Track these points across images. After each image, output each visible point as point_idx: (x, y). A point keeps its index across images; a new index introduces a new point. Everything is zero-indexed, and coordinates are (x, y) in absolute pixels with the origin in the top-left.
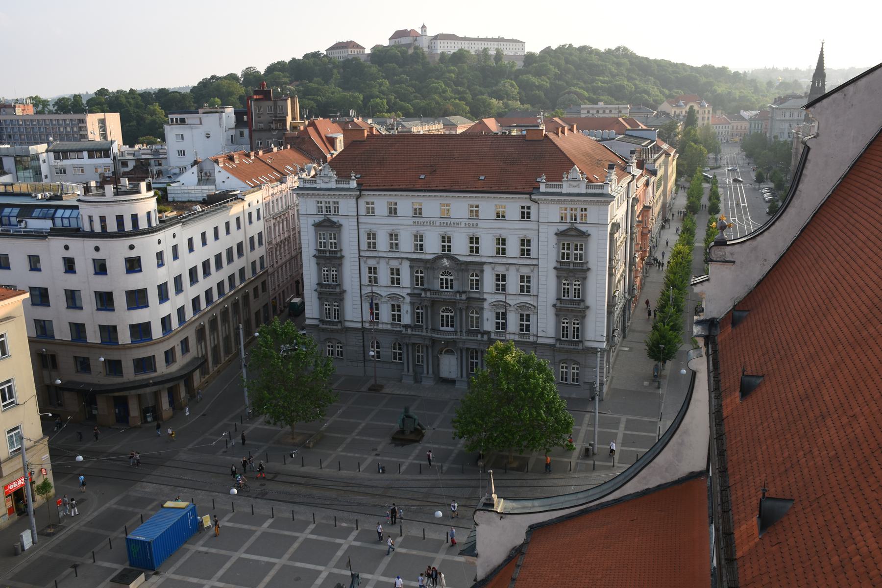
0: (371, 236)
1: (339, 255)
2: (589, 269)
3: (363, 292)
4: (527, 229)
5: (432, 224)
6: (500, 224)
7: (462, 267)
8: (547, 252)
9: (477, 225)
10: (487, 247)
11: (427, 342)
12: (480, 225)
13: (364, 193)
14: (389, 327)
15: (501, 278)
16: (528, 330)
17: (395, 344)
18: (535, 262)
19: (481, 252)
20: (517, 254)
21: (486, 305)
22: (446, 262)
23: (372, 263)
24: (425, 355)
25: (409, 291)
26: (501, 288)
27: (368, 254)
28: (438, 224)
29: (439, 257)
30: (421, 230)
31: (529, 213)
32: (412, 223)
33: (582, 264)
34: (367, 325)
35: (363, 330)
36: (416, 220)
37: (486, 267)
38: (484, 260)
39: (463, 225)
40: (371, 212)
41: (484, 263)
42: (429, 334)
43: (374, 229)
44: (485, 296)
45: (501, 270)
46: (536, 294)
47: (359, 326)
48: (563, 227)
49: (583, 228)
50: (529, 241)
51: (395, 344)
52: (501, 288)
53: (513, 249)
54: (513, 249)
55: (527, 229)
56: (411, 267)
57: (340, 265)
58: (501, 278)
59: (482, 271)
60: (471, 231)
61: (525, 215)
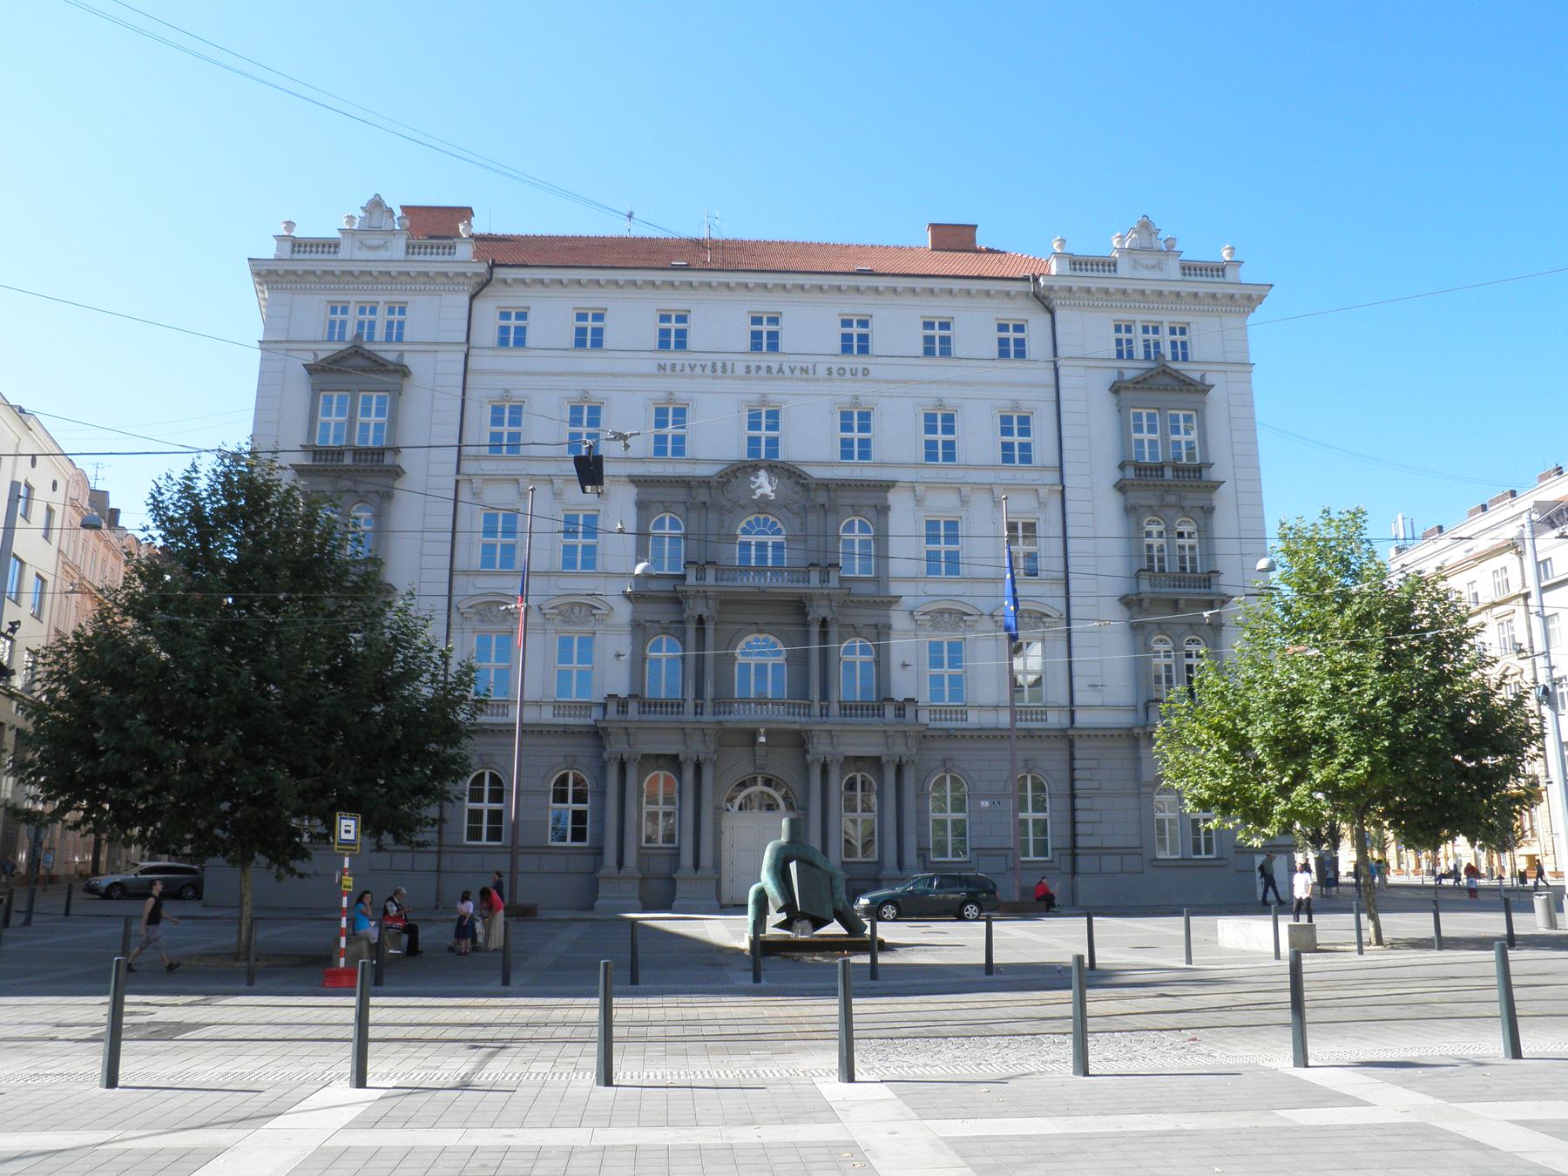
0: (509, 412)
1: (388, 459)
2: (1215, 486)
4: (1023, 384)
5: (721, 370)
6: (937, 368)
7: (814, 498)
8: (1093, 440)
9: (866, 372)
10: (897, 440)
11: (697, 748)
12: (875, 372)
13: (500, 273)
14: (547, 716)
15: (942, 531)
17: (563, 780)
19: (877, 453)
21: (899, 620)
22: (764, 485)
23: (500, 496)
26: (945, 564)
27: (489, 467)
28: (740, 369)
29: (741, 471)
30: (682, 388)
31: (1020, 343)
32: (651, 367)
33: (1199, 469)
36: (668, 357)
37: (893, 497)
38: (886, 475)
39: (822, 371)
40: (513, 337)
41: (888, 485)
44: (895, 589)
45: (942, 505)
48: (1132, 370)
49: (1191, 370)
50: (1024, 421)
52: (945, 564)
53: (978, 439)
54: (978, 439)
55: (1023, 384)
56: (642, 506)
57: (387, 496)
58: (942, 531)
59: (883, 510)
60: (845, 391)
61: (1011, 348)
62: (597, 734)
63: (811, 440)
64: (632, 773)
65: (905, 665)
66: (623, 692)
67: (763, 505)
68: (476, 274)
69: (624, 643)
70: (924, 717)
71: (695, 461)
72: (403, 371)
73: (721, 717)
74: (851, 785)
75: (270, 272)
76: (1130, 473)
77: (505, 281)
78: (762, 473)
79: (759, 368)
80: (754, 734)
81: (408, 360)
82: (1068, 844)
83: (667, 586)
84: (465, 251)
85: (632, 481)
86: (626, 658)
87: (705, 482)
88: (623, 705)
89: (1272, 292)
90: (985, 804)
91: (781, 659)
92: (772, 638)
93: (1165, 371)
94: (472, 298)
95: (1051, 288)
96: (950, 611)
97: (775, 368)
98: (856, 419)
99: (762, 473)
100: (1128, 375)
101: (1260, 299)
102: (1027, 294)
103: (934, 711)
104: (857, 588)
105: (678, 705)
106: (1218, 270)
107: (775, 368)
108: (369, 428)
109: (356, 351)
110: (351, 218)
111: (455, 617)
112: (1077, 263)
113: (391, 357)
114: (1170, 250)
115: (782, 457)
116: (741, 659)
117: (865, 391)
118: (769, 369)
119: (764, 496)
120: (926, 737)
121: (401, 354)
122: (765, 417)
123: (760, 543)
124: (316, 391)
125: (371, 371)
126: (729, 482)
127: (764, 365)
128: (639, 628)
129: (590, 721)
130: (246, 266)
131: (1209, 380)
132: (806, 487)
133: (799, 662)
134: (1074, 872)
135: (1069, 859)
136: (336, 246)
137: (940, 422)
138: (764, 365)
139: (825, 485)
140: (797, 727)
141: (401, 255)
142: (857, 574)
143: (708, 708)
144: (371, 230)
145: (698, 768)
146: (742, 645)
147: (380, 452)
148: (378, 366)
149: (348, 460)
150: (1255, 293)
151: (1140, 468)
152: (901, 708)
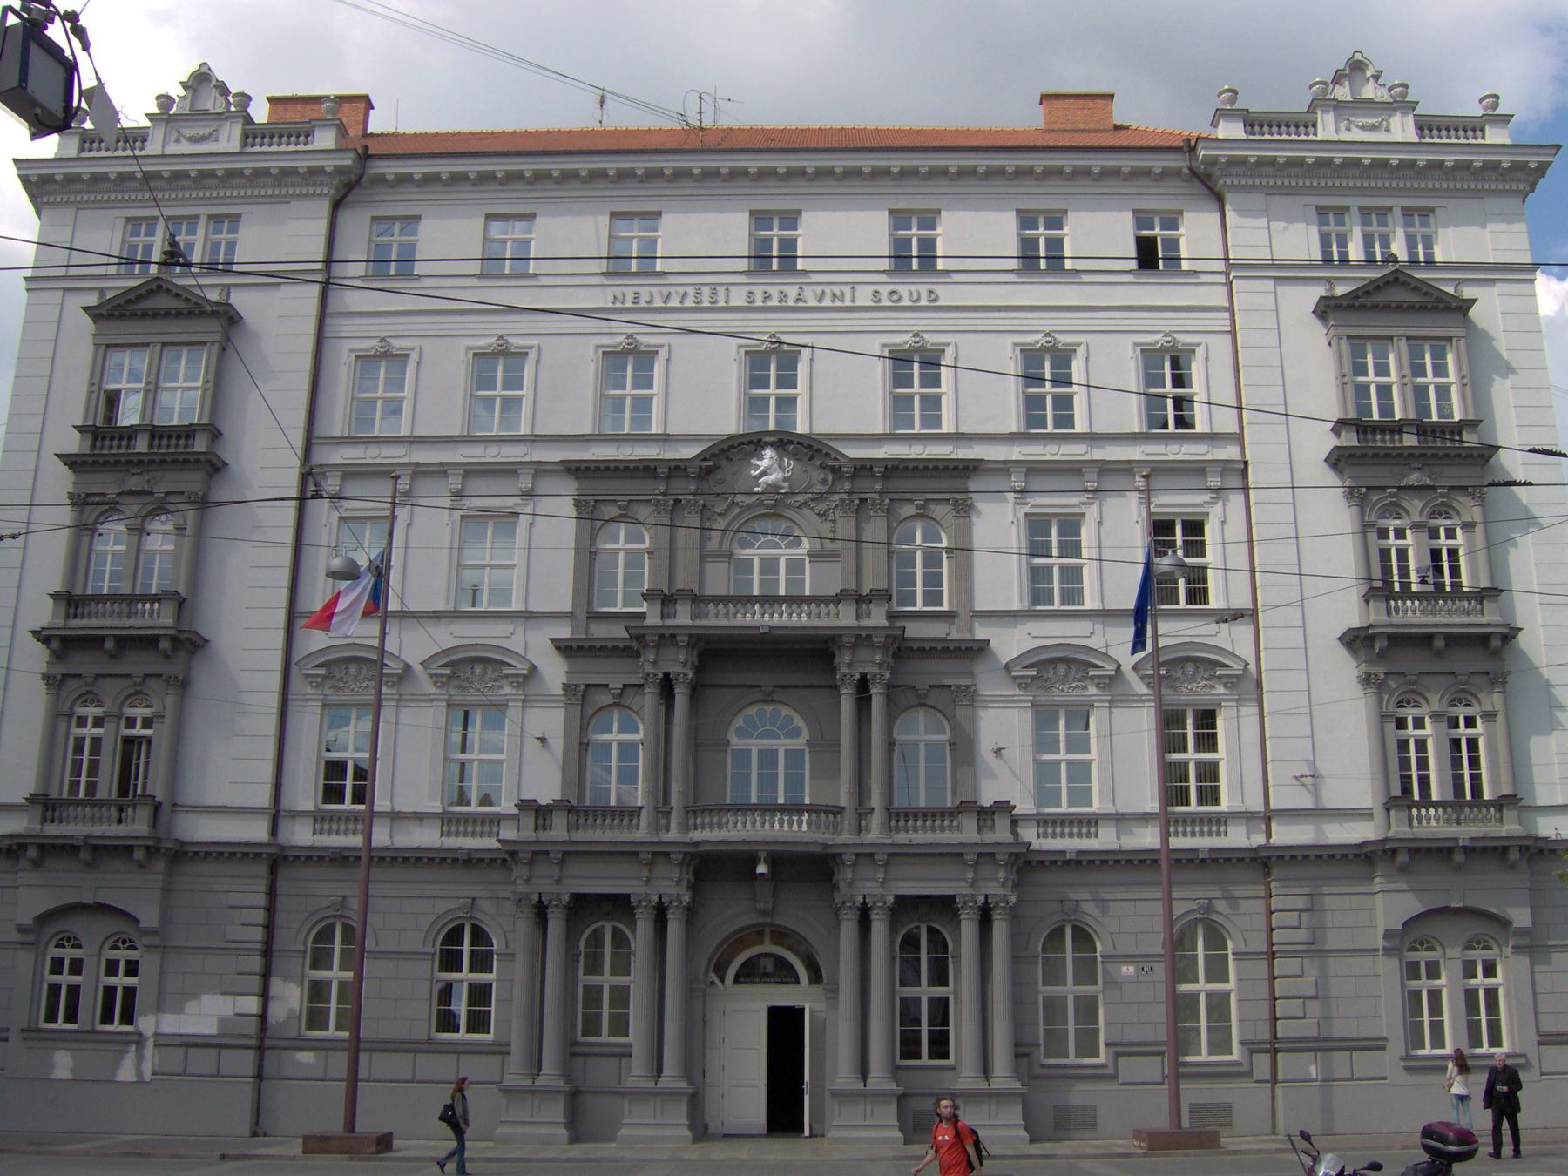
1: (200, 444)
3: (299, 653)
14: (427, 837)
16: (1210, 794)
17: (454, 936)
18: (1230, 452)
20: (1132, 417)
24: (637, 981)
25: (564, 631)
34: (301, 835)
35: (277, 861)
42: (673, 835)
43: (400, 335)
44: (981, 633)
46: (1243, 602)
47: (257, 831)
51: (454, 936)
62: (506, 858)
63: (843, 398)
64: (556, 925)
65: (998, 751)
66: (544, 800)
67: (775, 505)
68: (339, 170)
69: (551, 721)
70: (1029, 834)
71: (665, 438)
72: (229, 318)
73: (697, 835)
74: (911, 943)
75: (46, 180)
76: (1350, 439)
77: (381, 180)
78: (769, 453)
79: (767, 297)
80: (752, 860)
81: (238, 300)
82: (1265, 1035)
83: (618, 631)
84: (325, 139)
85: (569, 470)
86: (557, 743)
87: (677, 469)
88: (540, 813)
89: (1558, 161)
90: (1128, 970)
91: (800, 743)
92: (785, 711)
93: (1397, 279)
94: (337, 205)
95: (1212, 162)
96: (1066, 661)
97: (792, 292)
98: (914, 364)
99: (769, 453)
100: (1340, 290)
101: (1542, 169)
102: (1177, 173)
103: (1043, 821)
104: (915, 630)
105: (635, 812)
106: (1474, 126)
107: (792, 292)
108: (181, 402)
109: (157, 287)
110: (165, 101)
111: (298, 686)
112: (1252, 122)
113: (214, 296)
114: (1401, 103)
115: (801, 428)
116: (736, 742)
117: (931, 329)
118: (783, 296)
119: (773, 489)
120: (1026, 863)
121: (228, 288)
122: (771, 363)
123: (784, 572)
124: (105, 347)
125: (179, 314)
126: (717, 467)
127: (774, 291)
128: (579, 695)
129: (492, 843)
130: (13, 171)
131: (1468, 292)
132: (836, 471)
133: (824, 744)
134: (1274, 1080)
135: (1266, 1058)
136: (144, 140)
137: (1045, 366)
138: (774, 291)
139: (863, 468)
140: (818, 849)
141: (235, 146)
142: (919, 607)
143: (674, 820)
144: (197, 115)
145: (661, 915)
146: (739, 722)
147: (188, 432)
148: (195, 310)
149: (141, 445)
150: (1533, 160)
151: (1362, 427)
152: (986, 815)
